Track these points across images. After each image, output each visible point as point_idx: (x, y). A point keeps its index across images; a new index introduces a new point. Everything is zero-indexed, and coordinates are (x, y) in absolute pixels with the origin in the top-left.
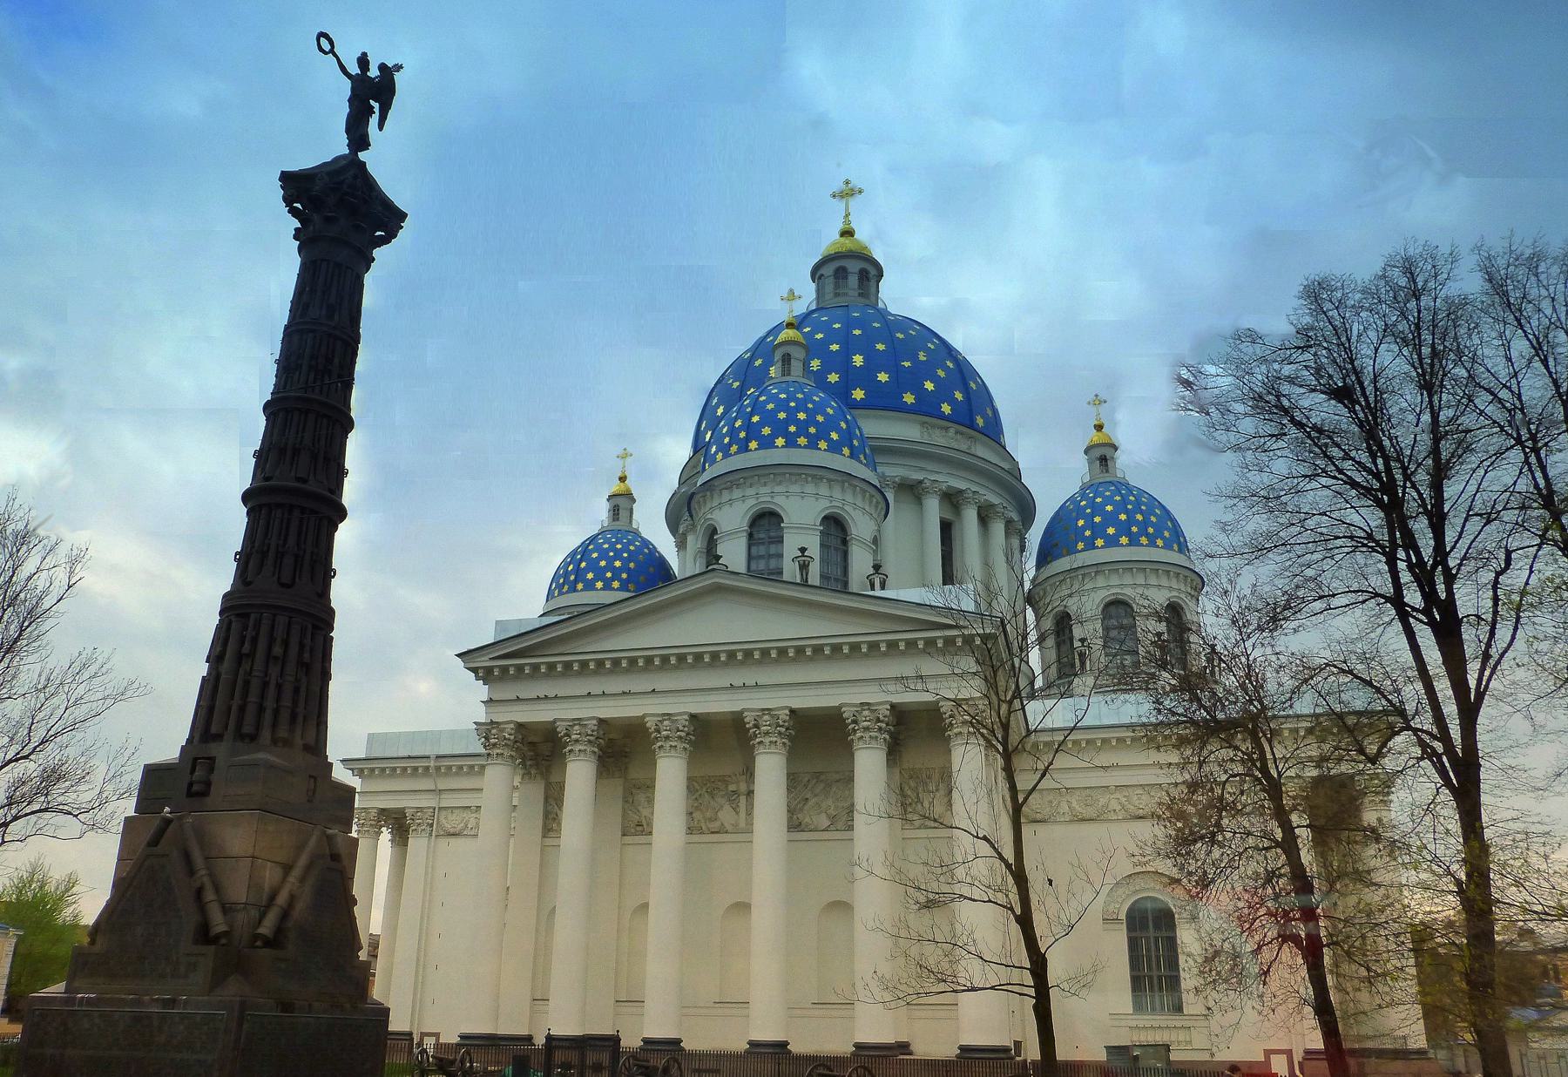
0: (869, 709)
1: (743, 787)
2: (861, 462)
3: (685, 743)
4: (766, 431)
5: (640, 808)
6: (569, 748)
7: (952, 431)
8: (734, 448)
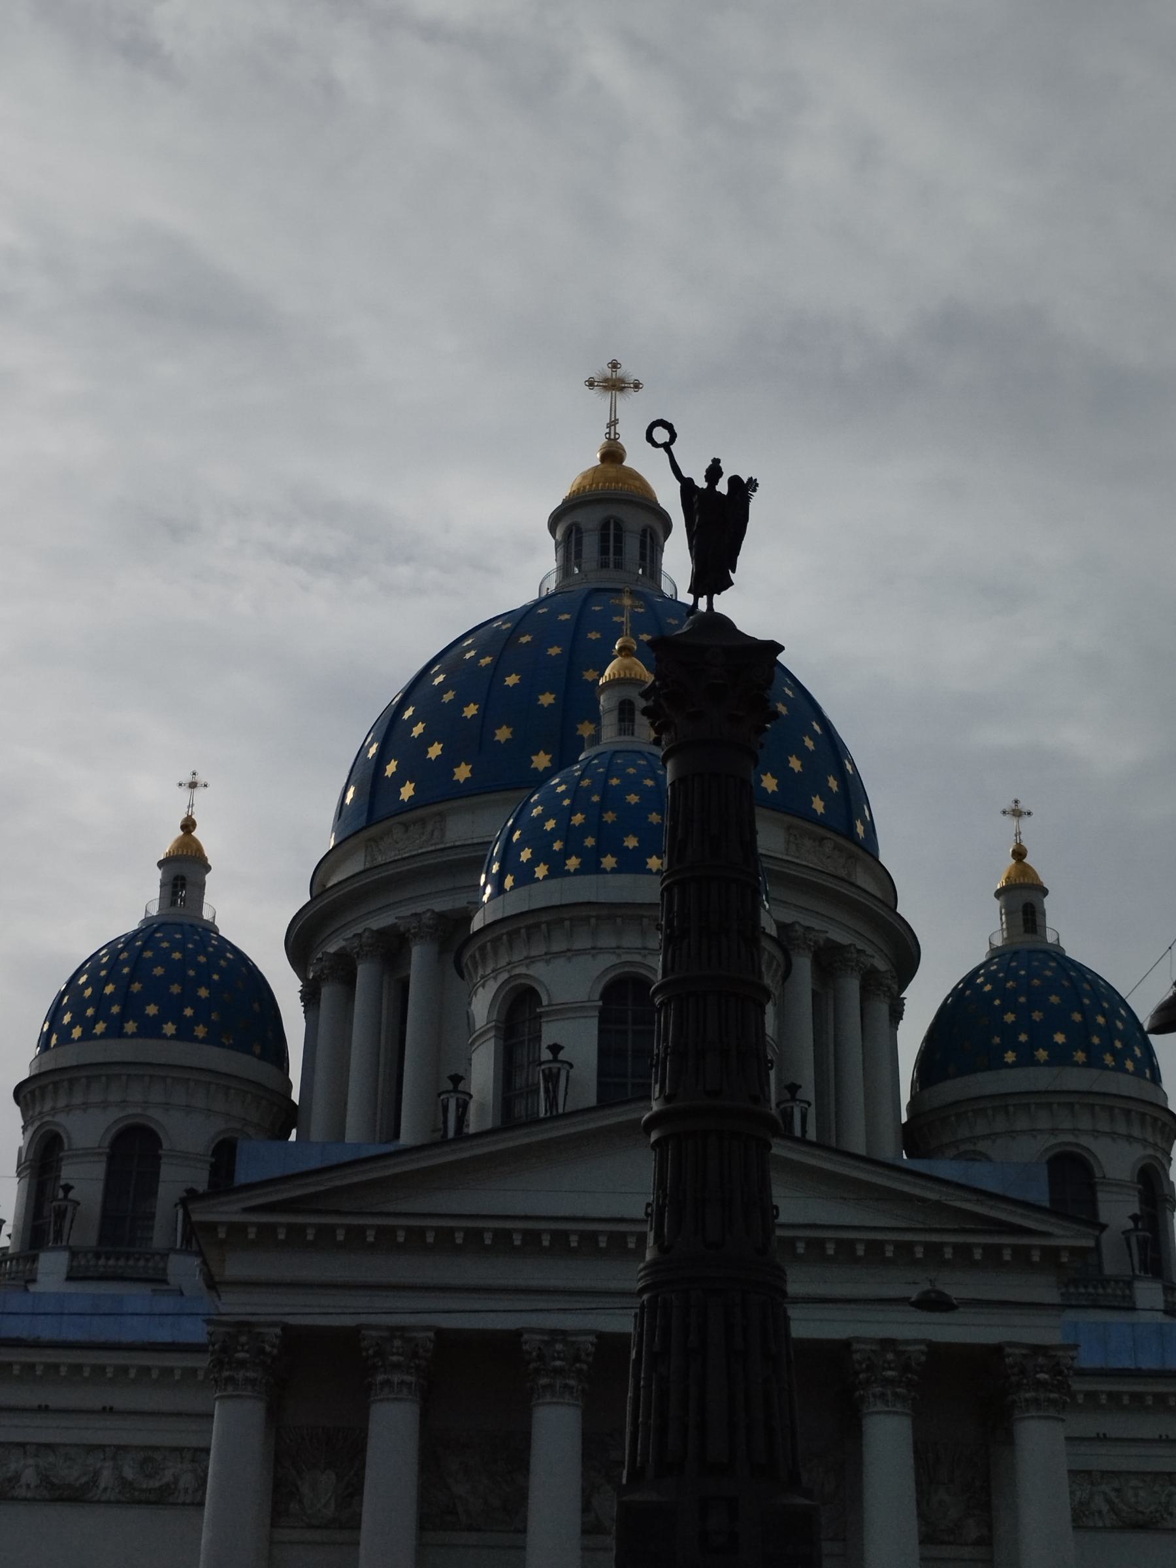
4: (631, 842)
8: (573, 863)
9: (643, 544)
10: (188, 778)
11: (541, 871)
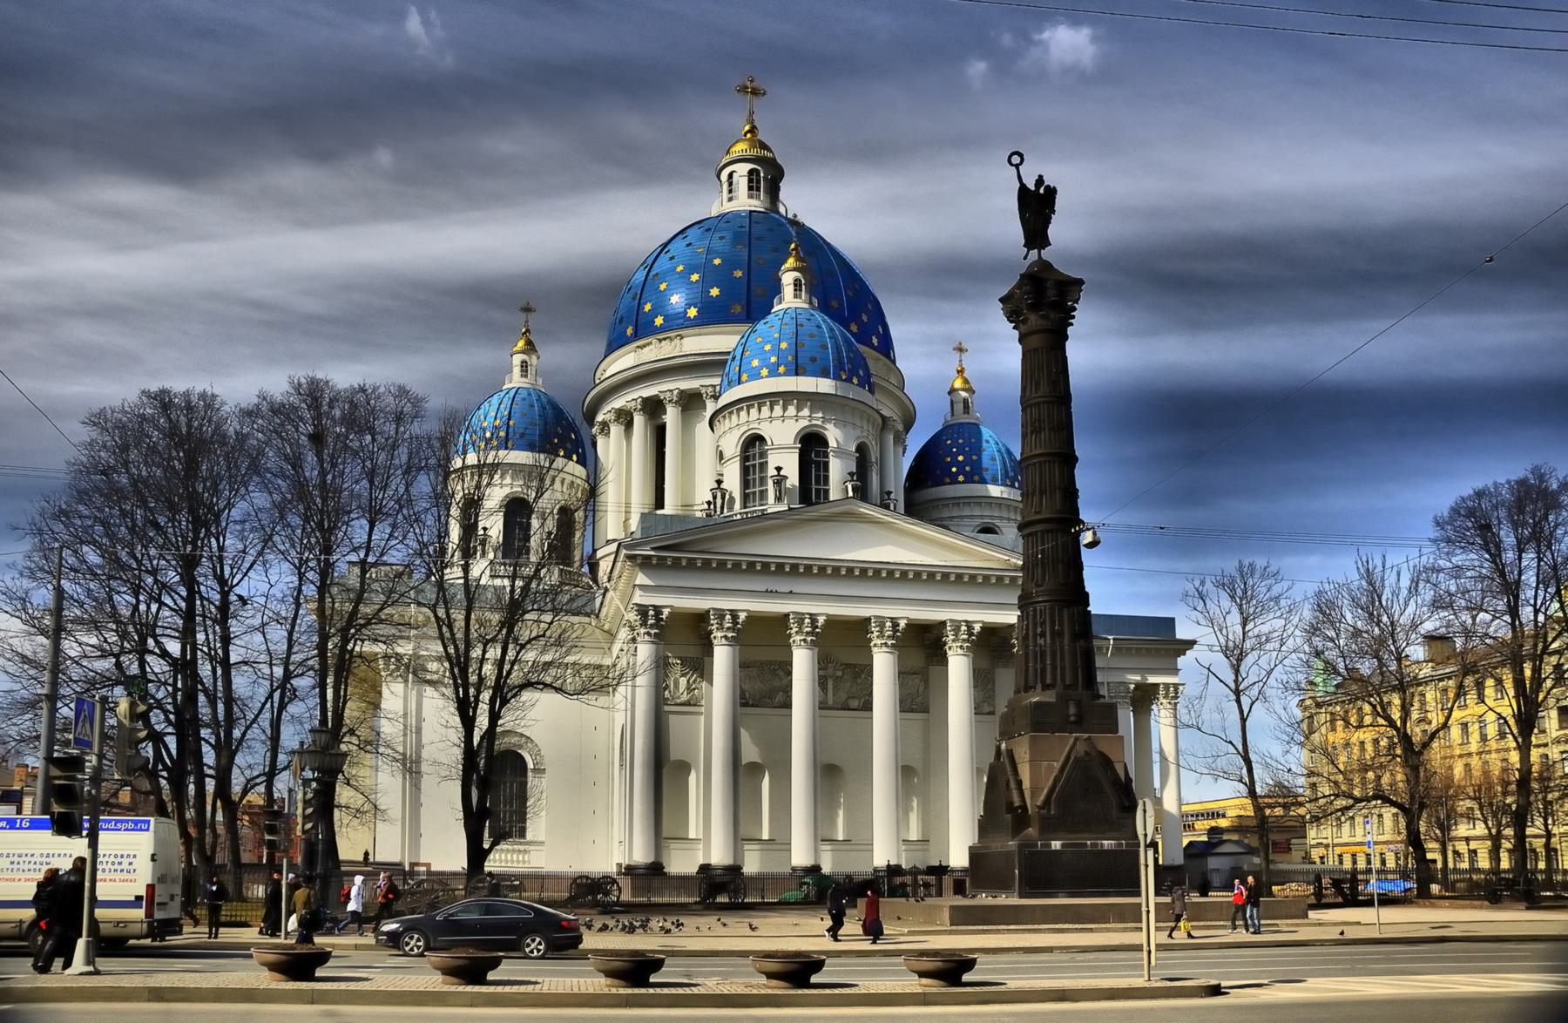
8: (782, 369)
11: (765, 372)
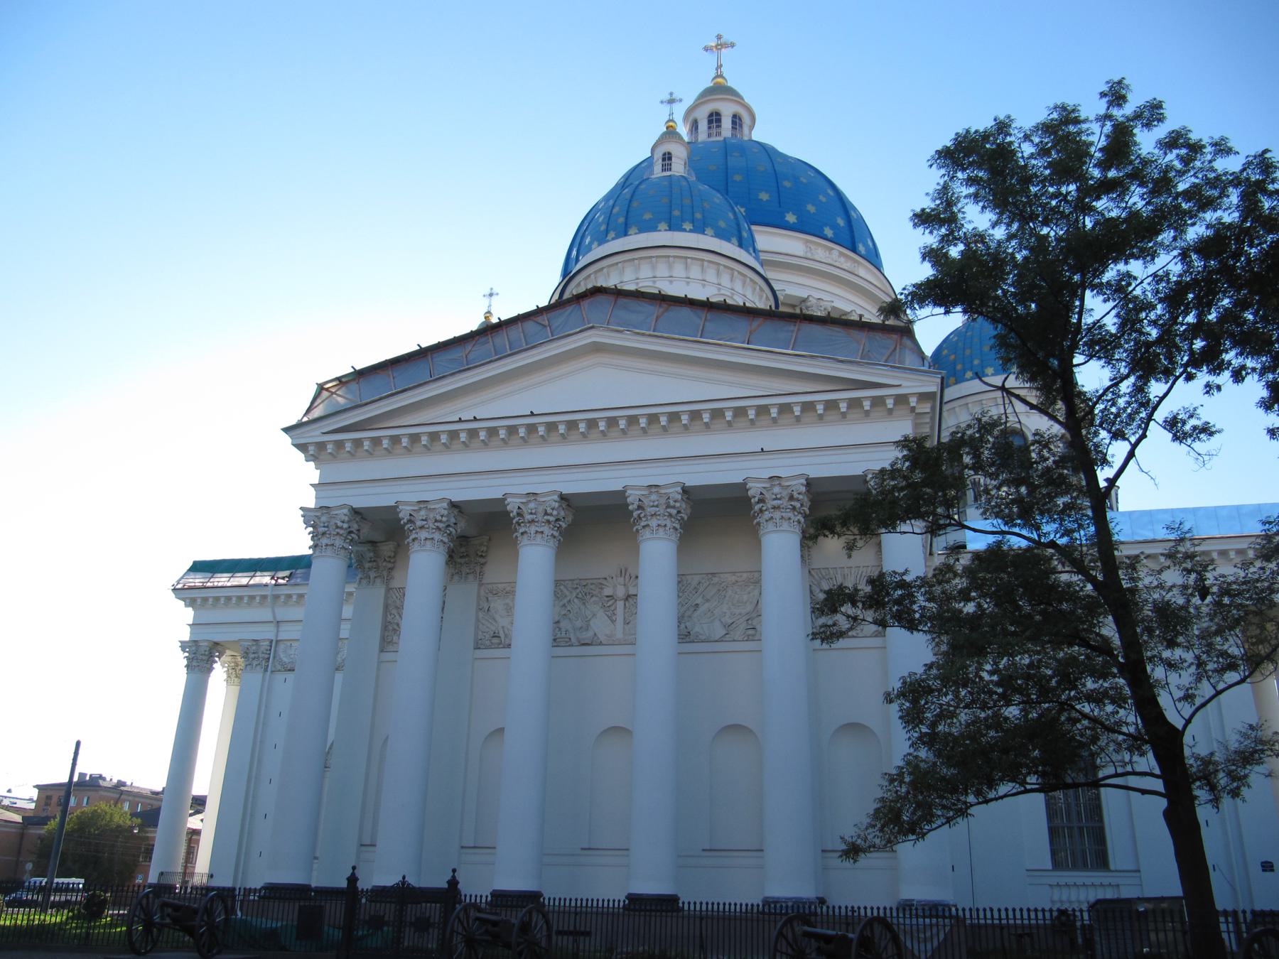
0: (780, 484)
1: (621, 592)
2: (751, 254)
3: (553, 529)
5: (497, 617)
6: (413, 536)
7: (835, 254)
9: (734, 123)
10: (488, 292)
